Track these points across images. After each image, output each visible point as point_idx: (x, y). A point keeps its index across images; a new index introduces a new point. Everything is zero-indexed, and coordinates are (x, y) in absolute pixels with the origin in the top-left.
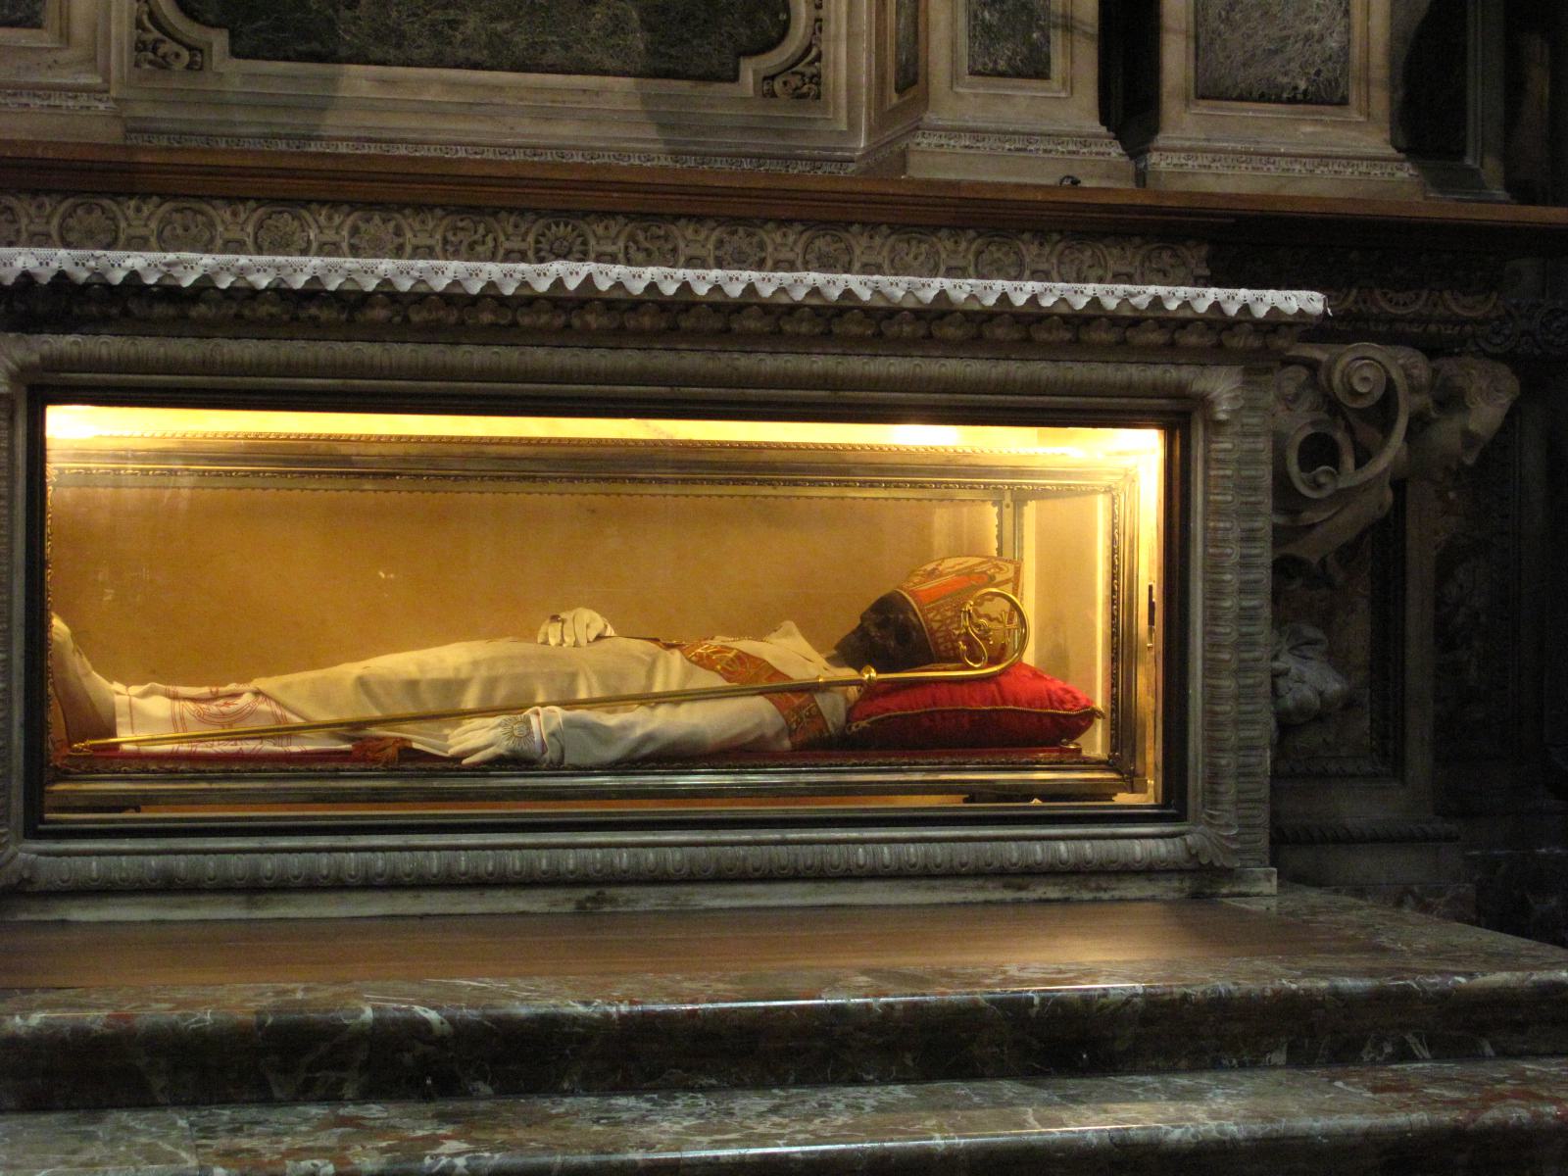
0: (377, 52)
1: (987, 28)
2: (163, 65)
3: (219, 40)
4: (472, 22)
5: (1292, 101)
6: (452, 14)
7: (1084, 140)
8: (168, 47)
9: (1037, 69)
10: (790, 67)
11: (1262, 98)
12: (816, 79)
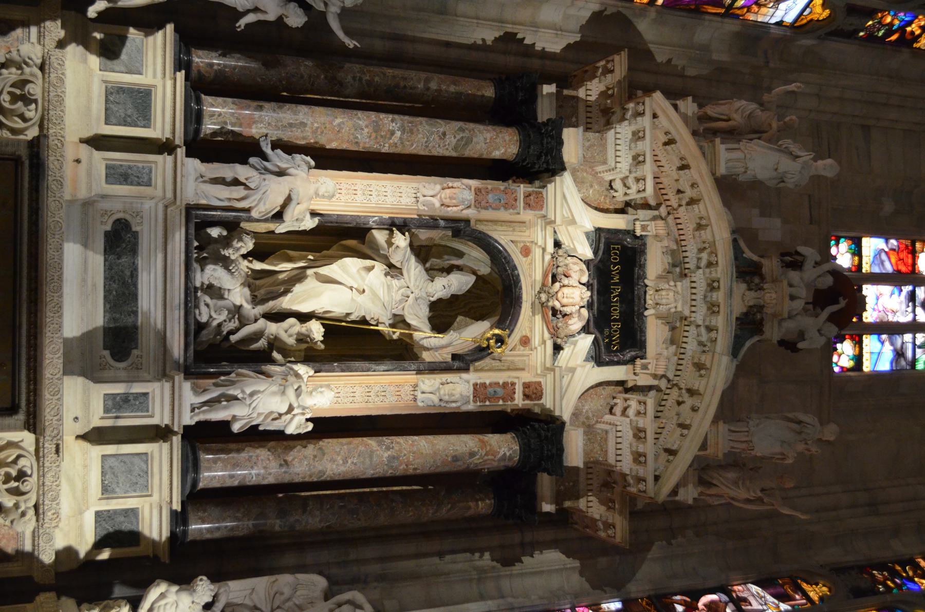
0: (107, 263)
1: (115, 398)
2: (102, 216)
3: (108, 227)
4: (115, 286)
5: (102, 481)
6: (117, 281)
7: (89, 422)
8: (107, 218)
9: (106, 410)
10: (107, 363)
11: (102, 472)
12: (104, 369)
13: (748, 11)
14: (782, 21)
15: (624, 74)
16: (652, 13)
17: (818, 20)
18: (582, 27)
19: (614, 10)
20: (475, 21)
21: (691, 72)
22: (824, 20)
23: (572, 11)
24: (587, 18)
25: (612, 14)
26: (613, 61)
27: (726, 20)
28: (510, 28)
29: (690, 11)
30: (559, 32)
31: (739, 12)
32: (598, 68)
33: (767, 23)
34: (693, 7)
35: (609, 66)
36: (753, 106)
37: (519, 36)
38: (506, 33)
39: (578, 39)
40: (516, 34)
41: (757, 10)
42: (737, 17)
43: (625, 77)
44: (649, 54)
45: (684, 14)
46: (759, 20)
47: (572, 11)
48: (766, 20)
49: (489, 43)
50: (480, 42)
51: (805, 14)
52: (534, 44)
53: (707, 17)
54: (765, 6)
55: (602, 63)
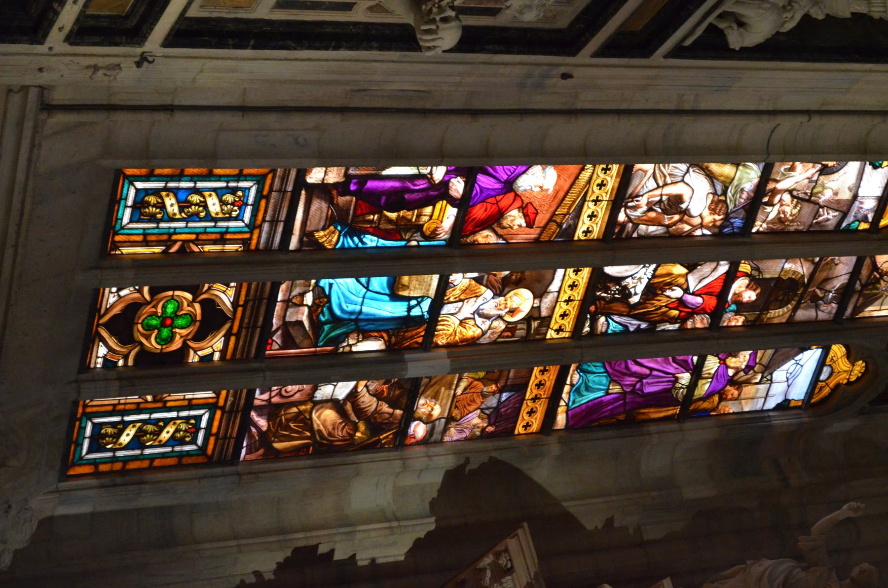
13: (721, 399)
14: (787, 401)
15: (532, 571)
16: (554, 447)
17: (849, 383)
18: (433, 503)
19: (484, 458)
20: (233, 543)
21: (653, 533)
22: (858, 379)
23: (408, 480)
24: (437, 487)
25: (482, 465)
26: (506, 550)
27: (688, 425)
28: (301, 539)
29: (620, 425)
30: (394, 524)
31: (706, 405)
32: (483, 570)
33: (762, 411)
34: (622, 417)
35: (503, 561)
36: (787, 565)
37: (323, 549)
38: (297, 551)
39: (432, 527)
40: (316, 547)
41: (736, 393)
42: (705, 414)
43: (536, 574)
44: (568, 520)
45: (610, 433)
46: (746, 409)
47: (408, 480)
48: (758, 405)
49: (268, 576)
50: (252, 579)
51: (823, 377)
52: (353, 556)
53: (653, 428)
54: (748, 382)
55: (488, 560)
